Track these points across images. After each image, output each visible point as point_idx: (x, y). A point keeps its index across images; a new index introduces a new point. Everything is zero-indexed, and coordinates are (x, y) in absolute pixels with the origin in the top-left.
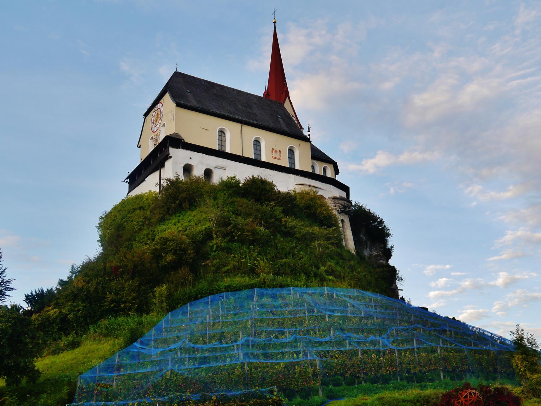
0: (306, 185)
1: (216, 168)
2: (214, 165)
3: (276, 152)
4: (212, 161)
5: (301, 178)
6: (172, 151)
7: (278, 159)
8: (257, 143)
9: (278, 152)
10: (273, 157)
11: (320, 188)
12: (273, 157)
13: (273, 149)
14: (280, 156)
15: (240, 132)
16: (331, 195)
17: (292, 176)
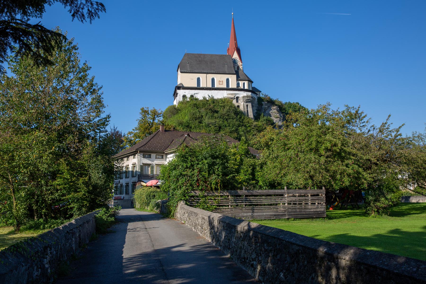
0: (231, 94)
1: (195, 94)
2: (194, 93)
3: (221, 81)
4: (192, 92)
5: (229, 91)
6: (178, 91)
7: (221, 84)
8: (213, 80)
9: (222, 82)
10: (219, 84)
11: (238, 94)
12: (219, 84)
13: (219, 81)
14: (223, 83)
15: (206, 77)
16: (242, 96)
17: (225, 91)
